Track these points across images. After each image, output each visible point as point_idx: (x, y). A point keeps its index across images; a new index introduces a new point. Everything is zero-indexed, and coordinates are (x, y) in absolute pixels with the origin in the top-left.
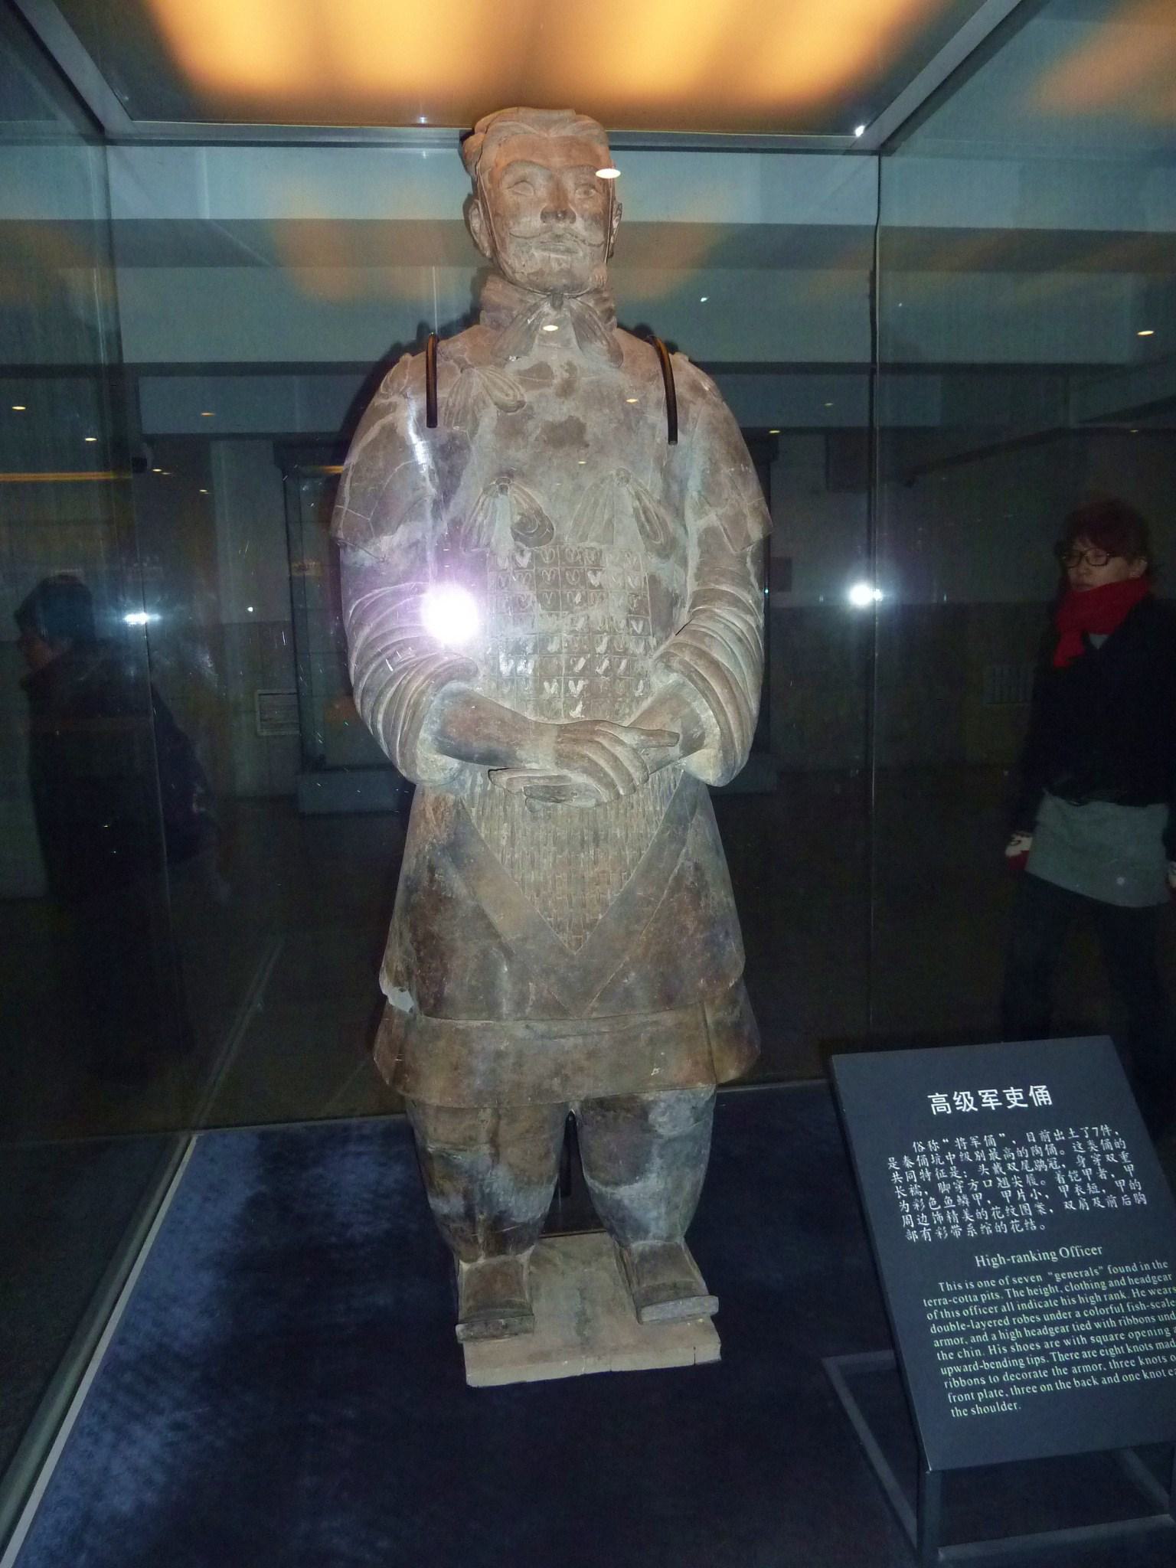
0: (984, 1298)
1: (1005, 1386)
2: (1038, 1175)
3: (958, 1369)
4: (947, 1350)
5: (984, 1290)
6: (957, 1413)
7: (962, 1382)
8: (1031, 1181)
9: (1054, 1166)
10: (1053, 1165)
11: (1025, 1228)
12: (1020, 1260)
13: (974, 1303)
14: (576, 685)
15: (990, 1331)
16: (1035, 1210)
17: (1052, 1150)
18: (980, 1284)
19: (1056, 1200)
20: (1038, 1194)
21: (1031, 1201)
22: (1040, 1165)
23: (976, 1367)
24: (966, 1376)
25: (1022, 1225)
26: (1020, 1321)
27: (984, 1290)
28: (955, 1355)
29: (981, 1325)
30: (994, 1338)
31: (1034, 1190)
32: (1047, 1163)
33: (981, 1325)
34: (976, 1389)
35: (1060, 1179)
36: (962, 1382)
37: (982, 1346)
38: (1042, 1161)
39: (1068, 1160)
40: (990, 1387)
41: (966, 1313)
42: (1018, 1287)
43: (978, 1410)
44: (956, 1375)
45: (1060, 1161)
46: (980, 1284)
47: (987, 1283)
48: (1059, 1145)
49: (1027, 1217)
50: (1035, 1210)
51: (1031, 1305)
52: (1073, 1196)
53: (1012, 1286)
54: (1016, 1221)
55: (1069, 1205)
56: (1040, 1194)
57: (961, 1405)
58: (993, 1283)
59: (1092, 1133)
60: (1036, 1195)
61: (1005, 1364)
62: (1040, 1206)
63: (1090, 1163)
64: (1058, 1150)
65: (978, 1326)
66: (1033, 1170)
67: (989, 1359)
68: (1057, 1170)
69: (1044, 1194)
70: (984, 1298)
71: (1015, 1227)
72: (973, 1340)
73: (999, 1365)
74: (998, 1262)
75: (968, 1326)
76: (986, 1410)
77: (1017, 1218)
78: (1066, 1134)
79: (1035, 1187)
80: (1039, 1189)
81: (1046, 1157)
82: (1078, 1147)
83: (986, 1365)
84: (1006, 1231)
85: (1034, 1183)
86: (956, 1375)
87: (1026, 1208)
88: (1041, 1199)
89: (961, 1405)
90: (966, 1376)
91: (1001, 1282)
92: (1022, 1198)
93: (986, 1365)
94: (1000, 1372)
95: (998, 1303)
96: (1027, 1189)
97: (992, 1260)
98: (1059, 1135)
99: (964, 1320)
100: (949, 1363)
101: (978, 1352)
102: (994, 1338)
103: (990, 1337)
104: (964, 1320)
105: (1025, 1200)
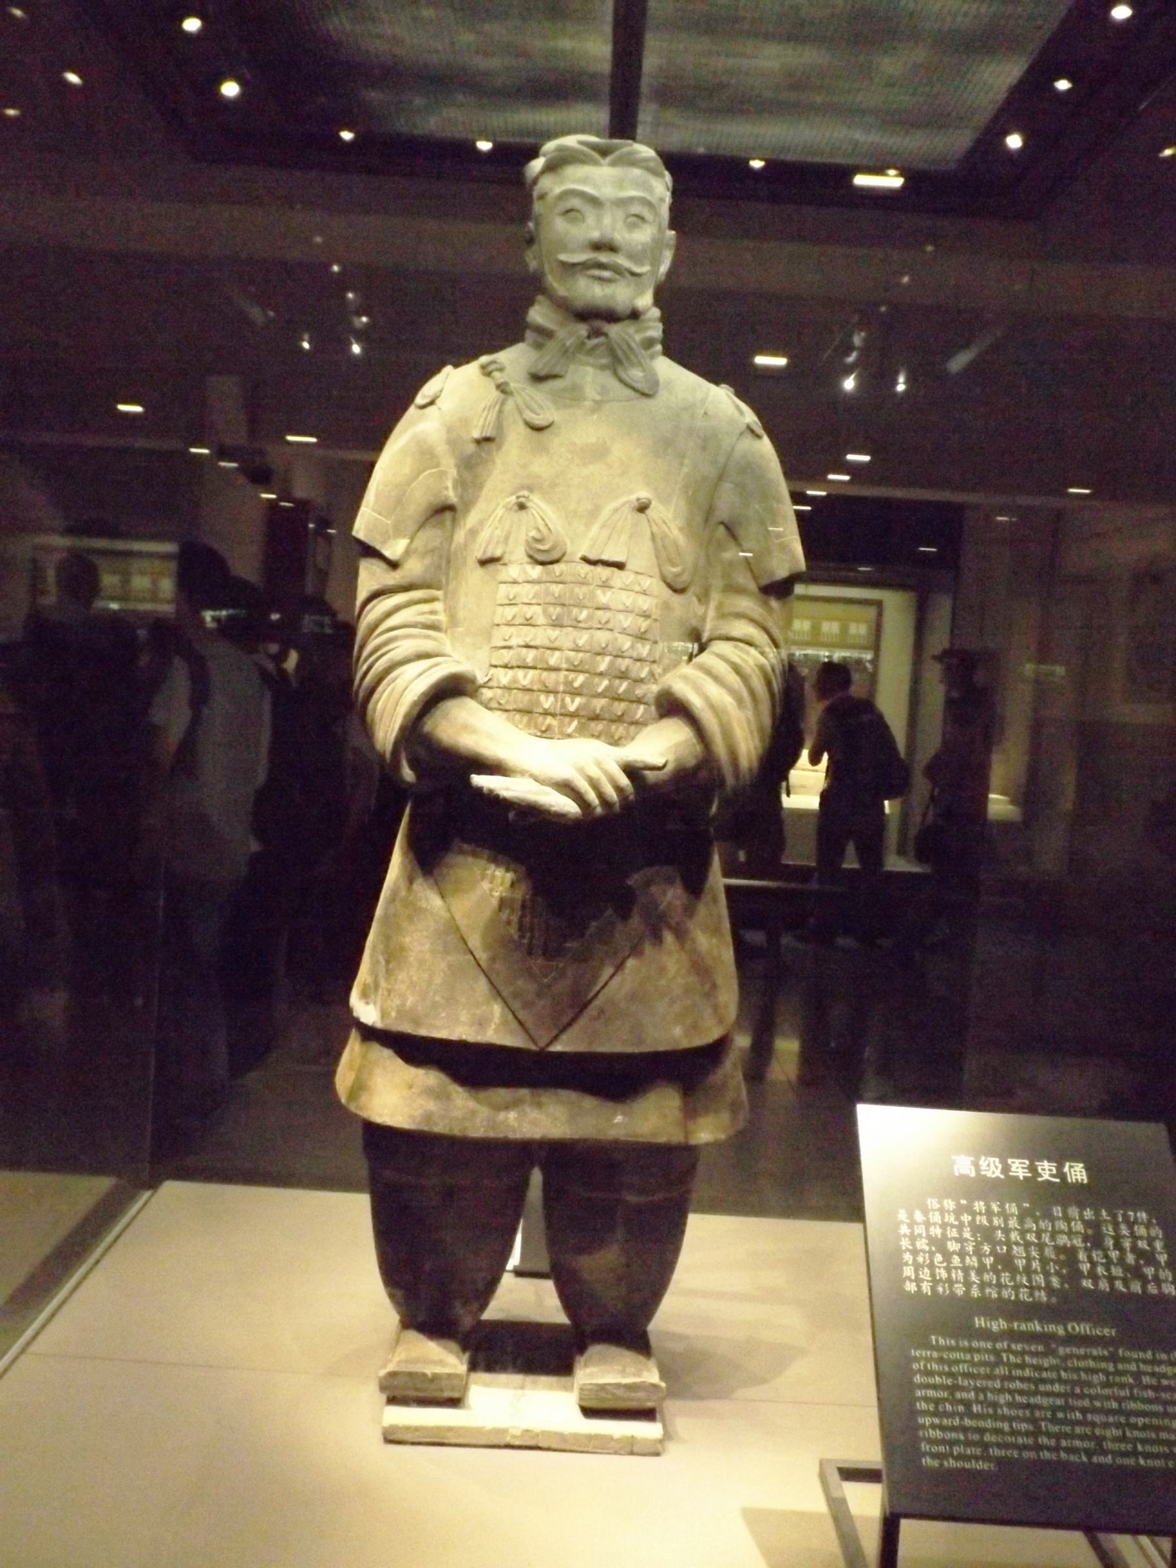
0: (977, 1358)
1: (986, 1446)
2: (1059, 1249)
3: (937, 1421)
4: (927, 1399)
5: (978, 1351)
6: (927, 1462)
7: (938, 1434)
8: (1049, 1253)
9: (1078, 1243)
10: (1078, 1242)
11: (1034, 1299)
12: (1023, 1327)
13: (965, 1362)
14: (573, 701)
15: (977, 1390)
16: (1048, 1283)
17: (1079, 1227)
18: (975, 1344)
19: (1075, 1275)
20: (1055, 1269)
21: (1047, 1274)
22: (1063, 1240)
23: (957, 1422)
24: (943, 1428)
25: (1031, 1295)
26: (1012, 1386)
27: (978, 1351)
28: (936, 1407)
29: (969, 1383)
30: (981, 1397)
31: (1052, 1264)
32: (1070, 1239)
33: (969, 1383)
34: (956, 1442)
35: (1082, 1256)
36: (938, 1434)
37: (967, 1404)
38: (1065, 1237)
39: (1095, 1240)
40: (968, 1444)
41: (954, 1369)
42: (1015, 1353)
43: (951, 1463)
44: (933, 1426)
45: (1086, 1238)
46: (975, 1344)
47: (983, 1344)
48: (1087, 1224)
49: (1039, 1288)
50: (1048, 1283)
51: (1027, 1373)
52: (1093, 1275)
53: (1009, 1350)
54: (1026, 1290)
55: (1087, 1284)
56: (1057, 1268)
57: (934, 1456)
58: (989, 1345)
59: (1125, 1216)
60: (1052, 1268)
61: (989, 1424)
62: (1055, 1282)
63: (1118, 1246)
64: (1085, 1228)
65: (966, 1383)
66: (1053, 1244)
67: (972, 1416)
68: (1080, 1248)
69: (1061, 1268)
70: (977, 1358)
71: (1023, 1295)
72: (958, 1395)
73: (981, 1424)
74: (999, 1326)
75: (956, 1382)
76: (960, 1464)
77: (1026, 1287)
78: (1097, 1213)
79: (1052, 1260)
80: (1055, 1262)
81: (1070, 1233)
82: (1109, 1230)
83: (968, 1422)
84: (1013, 1298)
85: (1053, 1257)
86: (933, 1426)
87: (1040, 1279)
88: (1058, 1273)
89: (934, 1456)
90: (943, 1428)
91: (999, 1346)
92: (1036, 1269)
93: (968, 1422)
94: (981, 1431)
95: (994, 1365)
96: (1044, 1261)
97: (993, 1324)
98: (1088, 1214)
99: (951, 1375)
100: (925, 1413)
101: (961, 1408)
102: (981, 1397)
103: (977, 1395)
104: (951, 1375)
105: (1039, 1270)
